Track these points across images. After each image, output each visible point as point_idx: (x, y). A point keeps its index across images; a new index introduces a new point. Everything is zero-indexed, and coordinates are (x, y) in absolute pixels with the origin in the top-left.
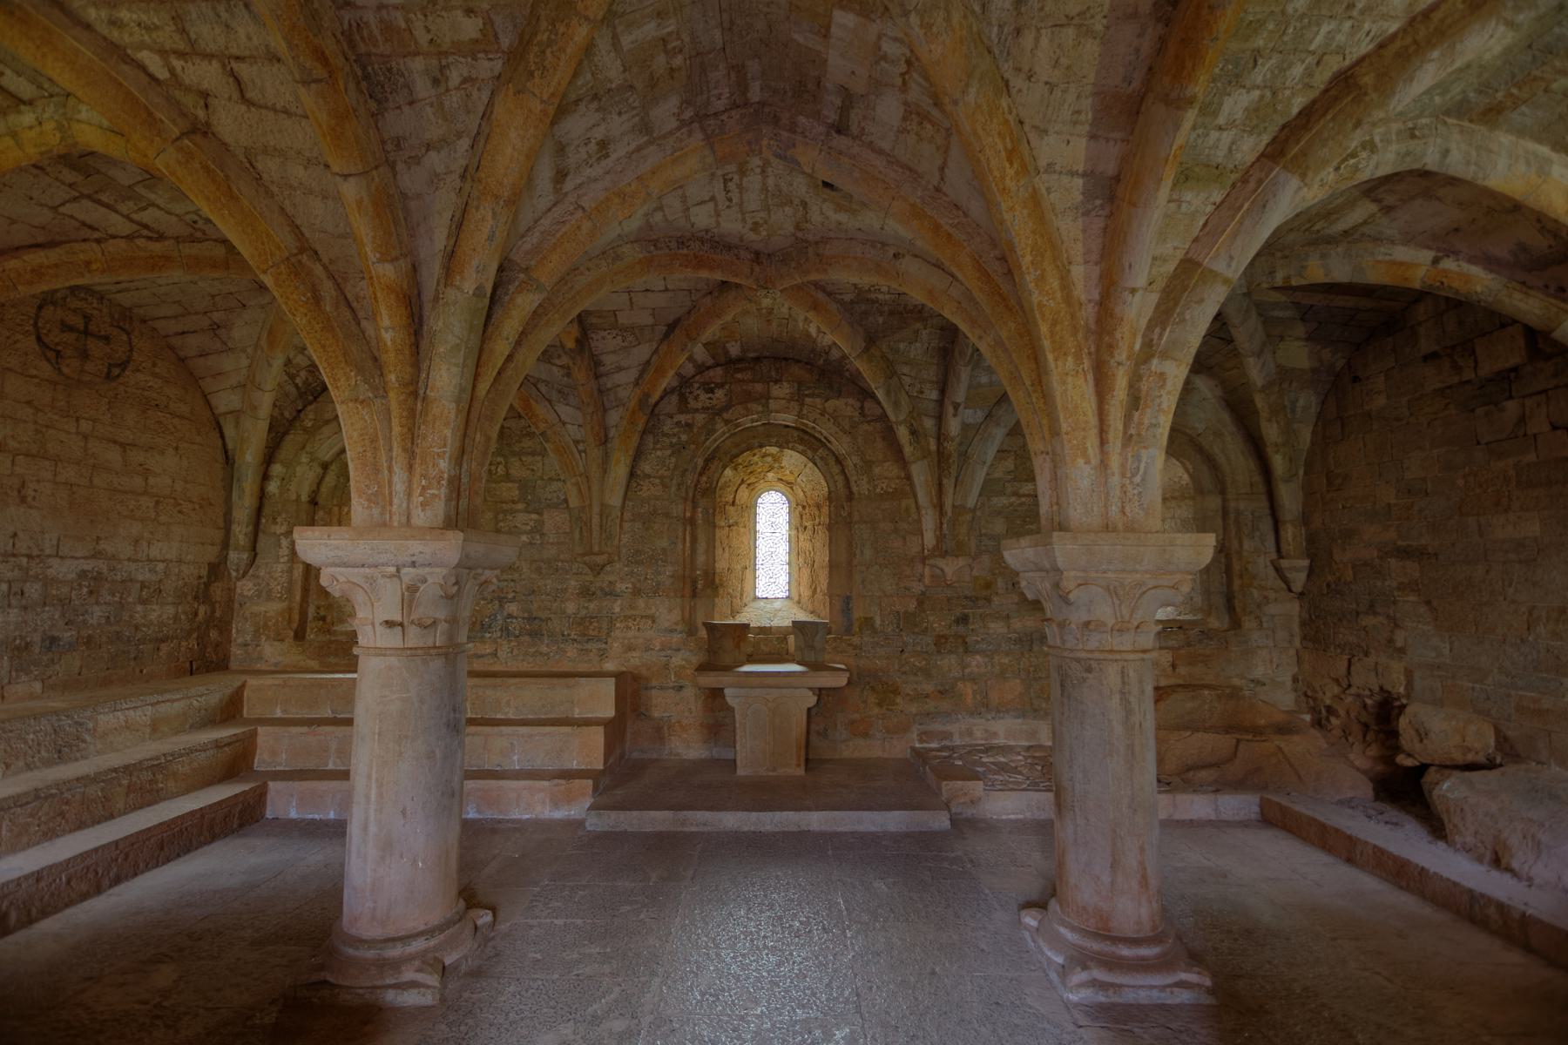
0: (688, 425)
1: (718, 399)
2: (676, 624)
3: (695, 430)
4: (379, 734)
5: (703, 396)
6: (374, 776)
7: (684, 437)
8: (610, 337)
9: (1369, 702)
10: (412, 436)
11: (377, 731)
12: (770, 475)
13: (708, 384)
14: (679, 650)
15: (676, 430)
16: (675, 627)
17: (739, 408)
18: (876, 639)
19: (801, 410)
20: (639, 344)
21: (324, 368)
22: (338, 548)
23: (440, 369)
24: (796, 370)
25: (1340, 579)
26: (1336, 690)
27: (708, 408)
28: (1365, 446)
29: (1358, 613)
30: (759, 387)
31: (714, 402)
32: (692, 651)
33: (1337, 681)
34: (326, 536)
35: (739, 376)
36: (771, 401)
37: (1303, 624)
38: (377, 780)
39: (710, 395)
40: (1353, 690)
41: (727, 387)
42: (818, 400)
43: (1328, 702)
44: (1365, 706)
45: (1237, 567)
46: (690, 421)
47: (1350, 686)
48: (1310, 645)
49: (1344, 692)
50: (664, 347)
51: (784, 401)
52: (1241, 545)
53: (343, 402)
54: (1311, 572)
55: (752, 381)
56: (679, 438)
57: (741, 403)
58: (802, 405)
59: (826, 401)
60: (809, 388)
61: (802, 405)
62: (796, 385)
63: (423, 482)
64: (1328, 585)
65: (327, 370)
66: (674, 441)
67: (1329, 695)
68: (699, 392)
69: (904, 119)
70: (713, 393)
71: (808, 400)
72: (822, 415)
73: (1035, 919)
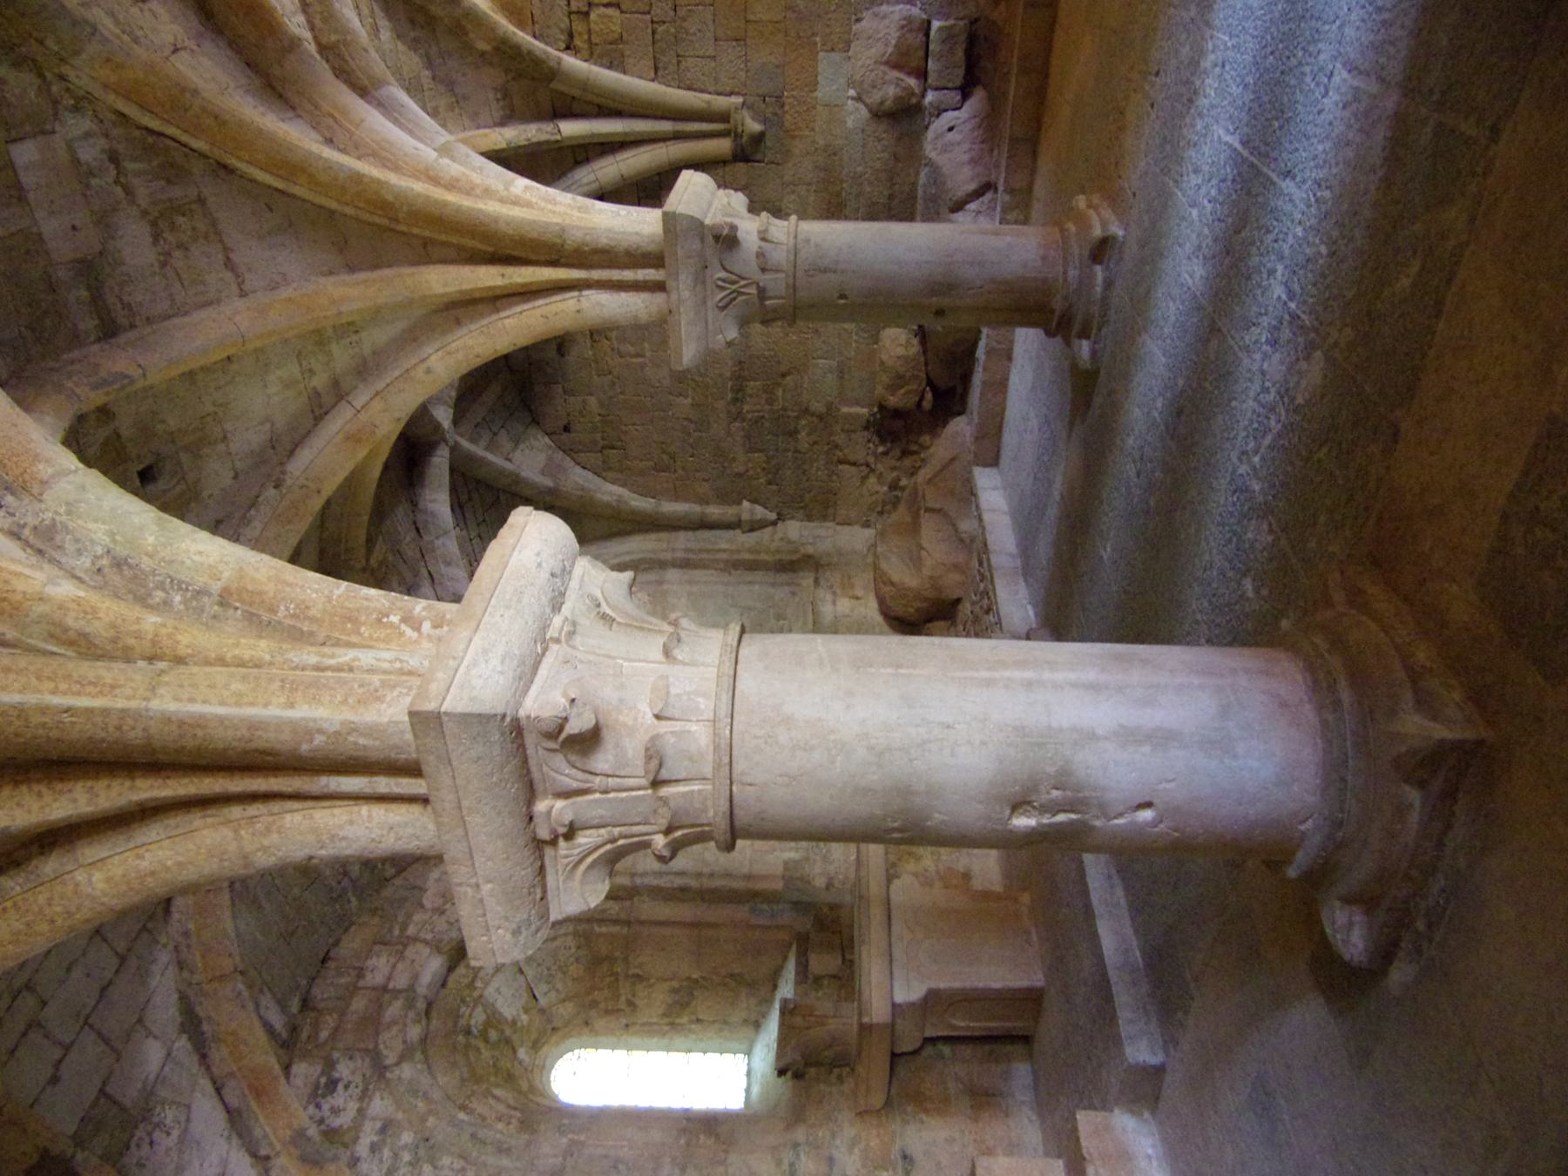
0: (383, 1131)
1: (353, 1073)
2: (779, 1163)
3: (400, 1116)
4: (899, 666)
5: (339, 1099)
6: (984, 674)
7: (407, 1137)
8: (146, 1148)
9: (881, 449)
10: (297, 632)
11: (890, 670)
12: (522, 1053)
13: (317, 1087)
14: (831, 1160)
15: (386, 1153)
16: (785, 1167)
17: (385, 1036)
18: (818, 858)
19: (426, 942)
20: (188, 1107)
21: (54, 692)
22: (485, 652)
23: (188, 551)
24: (350, 945)
25: (764, 469)
26: (872, 480)
27: (365, 1090)
28: (634, 424)
29: (797, 451)
30: (359, 1004)
31: (358, 1079)
32: (833, 1136)
33: (864, 478)
34: (452, 663)
35: (324, 1035)
36: (391, 986)
37: (810, 518)
38: (989, 669)
39: (340, 1086)
40: (871, 459)
41: (336, 1055)
42: (417, 917)
43: (885, 488)
44: (885, 454)
45: (747, 556)
46: (379, 1125)
47: (868, 465)
48: (831, 511)
49: (873, 470)
50: (218, 1054)
51: (400, 966)
52: (725, 551)
53: (153, 689)
54: (754, 501)
55: (343, 1014)
56: (405, 1147)
57: (377, 1033)
58: (416, 939)
59: (422, 906)
60: (390, 930)
61: (416, 939)
62: (377, 948)
63: (394, 619)
64: (769, 483)
65: (63, 686)
66: (406, 1157)
67: (878, 488)
68: (326, 1107)
69: (156, 237)
70: (338, 1080)
71: (411, 930)
72: (443, 912)
73: (1080, 346)
